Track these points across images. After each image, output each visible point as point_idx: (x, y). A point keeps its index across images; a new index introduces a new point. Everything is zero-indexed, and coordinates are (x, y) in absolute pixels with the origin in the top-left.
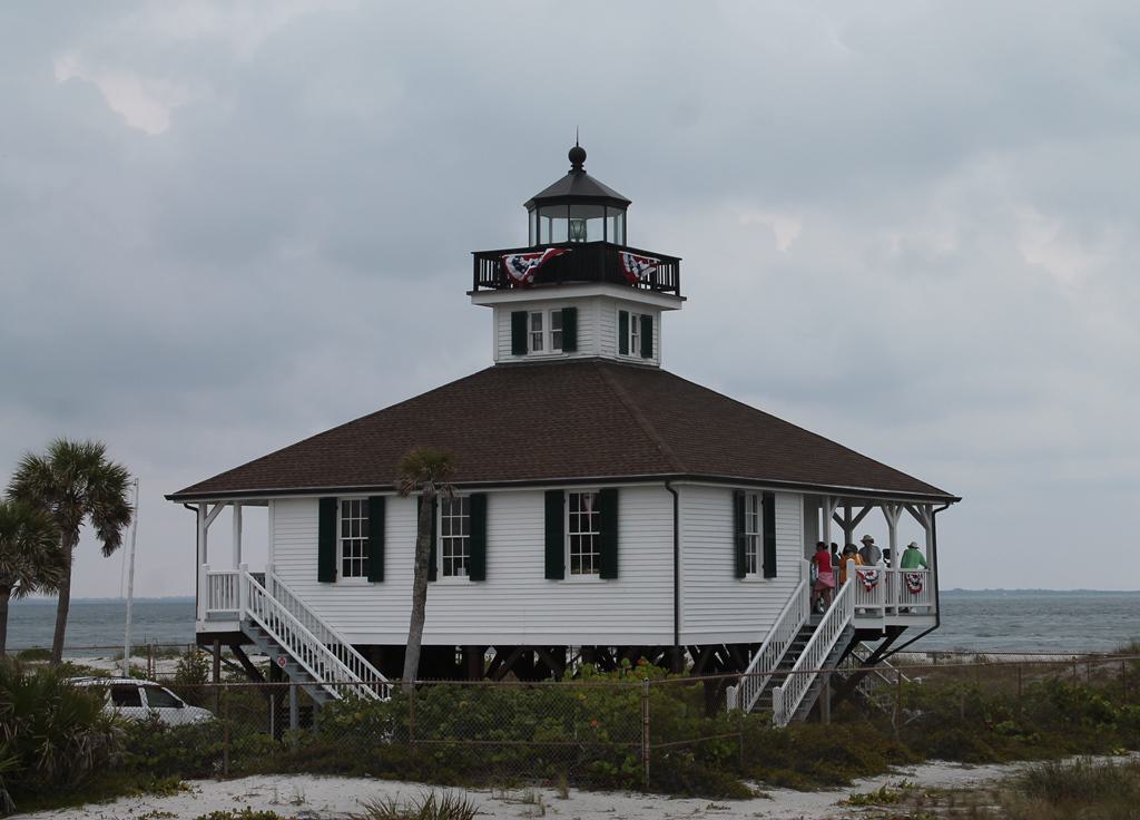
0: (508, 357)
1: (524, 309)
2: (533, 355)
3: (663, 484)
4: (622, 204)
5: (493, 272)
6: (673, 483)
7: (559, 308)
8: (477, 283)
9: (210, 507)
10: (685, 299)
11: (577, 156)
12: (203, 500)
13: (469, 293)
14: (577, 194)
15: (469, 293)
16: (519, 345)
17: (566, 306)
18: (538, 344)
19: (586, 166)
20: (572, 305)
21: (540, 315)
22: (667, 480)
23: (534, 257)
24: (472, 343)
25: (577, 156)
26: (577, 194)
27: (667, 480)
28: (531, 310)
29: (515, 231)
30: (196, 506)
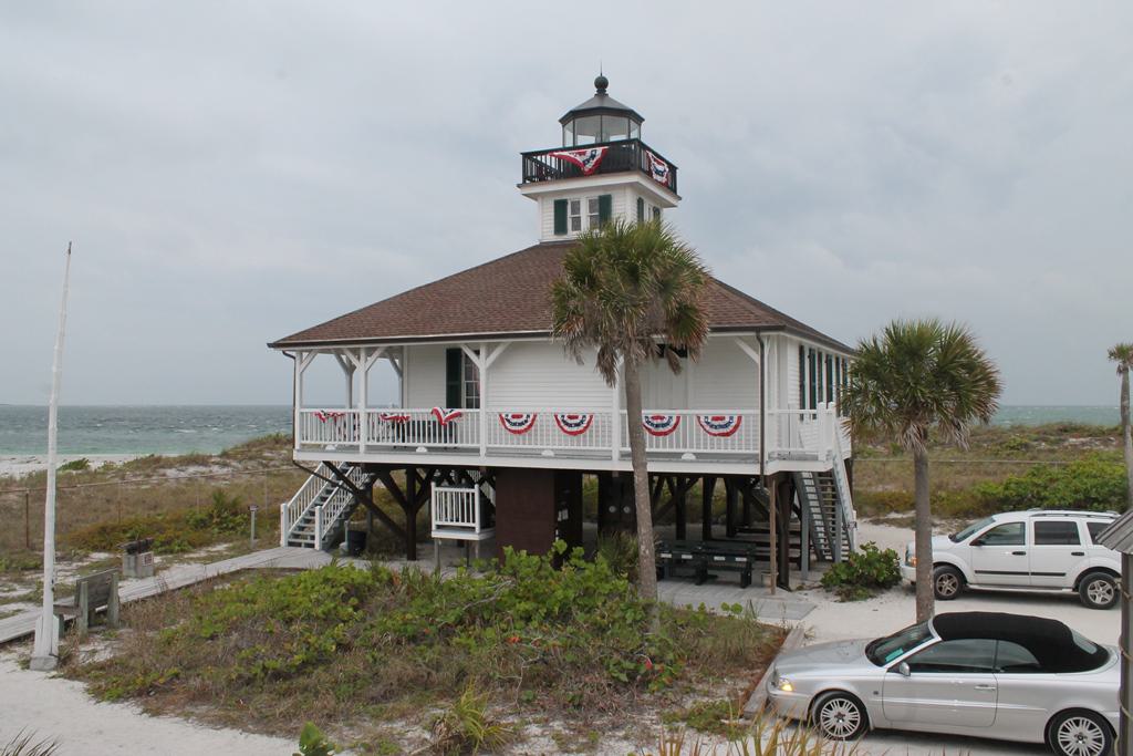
0: (551, 237)
1: (564, 198)
2: (572, 235)
3: (753, 334)
4: (639, 120)
5: (535, 169)
6: (762, 334)
7: (595, 195)
8: (525, 178)
9: (305, 354)
10: (680, 198)
11: (602, 84)
12: (296, 348)
13: (519, 186)
14: (601, 110)
15: (519, 186)
16: (560, 227)
17: (602, 193)
18: (577, 226)
19: (608, 90)
20: (608, 193)
21: (579, 202)
22: (758, 330)
23: (580, 154)
24: (518, 224)
25: (602, 84)
26: (601, 110)
27: (758, 330)
28: (570, 198)
29: (551, 137)
30: (294, 354)
